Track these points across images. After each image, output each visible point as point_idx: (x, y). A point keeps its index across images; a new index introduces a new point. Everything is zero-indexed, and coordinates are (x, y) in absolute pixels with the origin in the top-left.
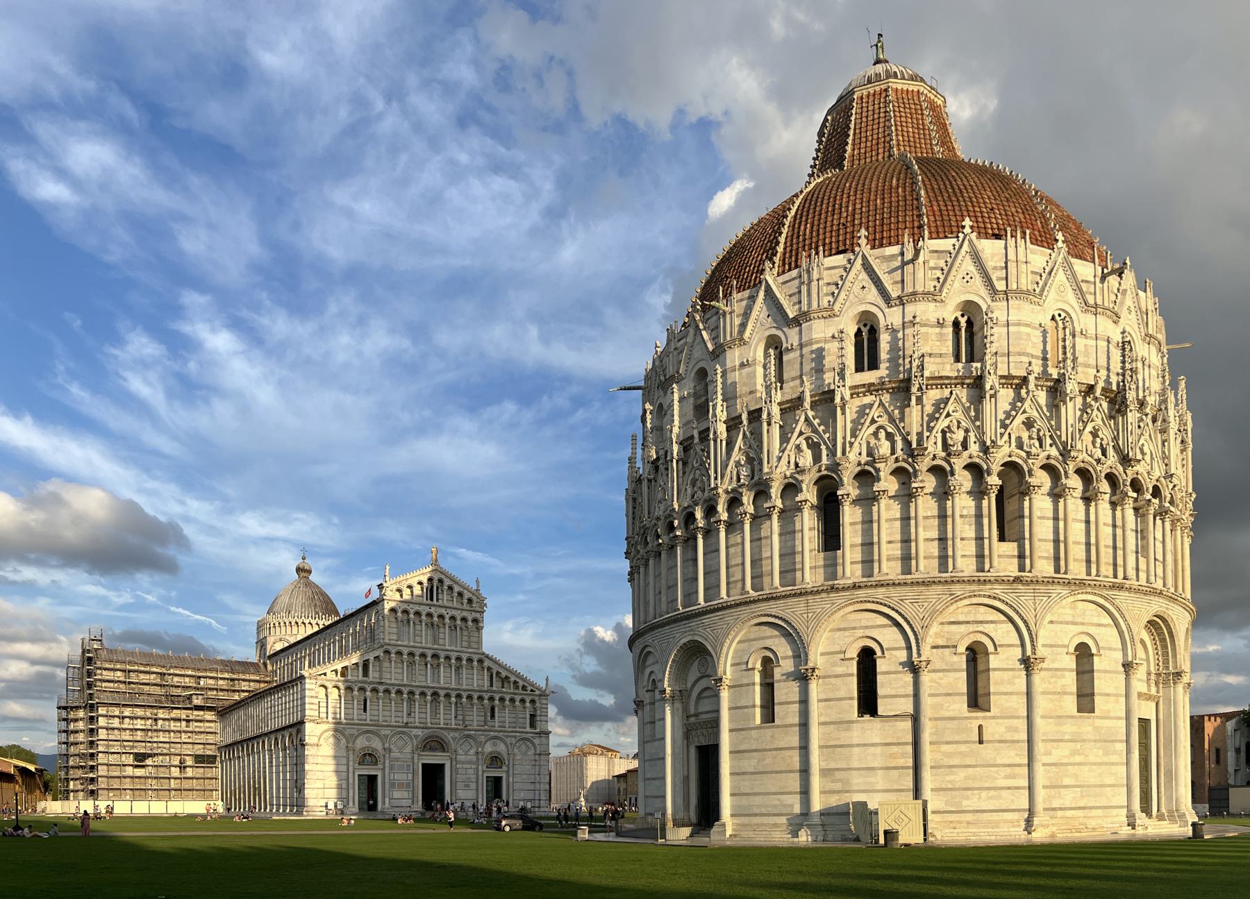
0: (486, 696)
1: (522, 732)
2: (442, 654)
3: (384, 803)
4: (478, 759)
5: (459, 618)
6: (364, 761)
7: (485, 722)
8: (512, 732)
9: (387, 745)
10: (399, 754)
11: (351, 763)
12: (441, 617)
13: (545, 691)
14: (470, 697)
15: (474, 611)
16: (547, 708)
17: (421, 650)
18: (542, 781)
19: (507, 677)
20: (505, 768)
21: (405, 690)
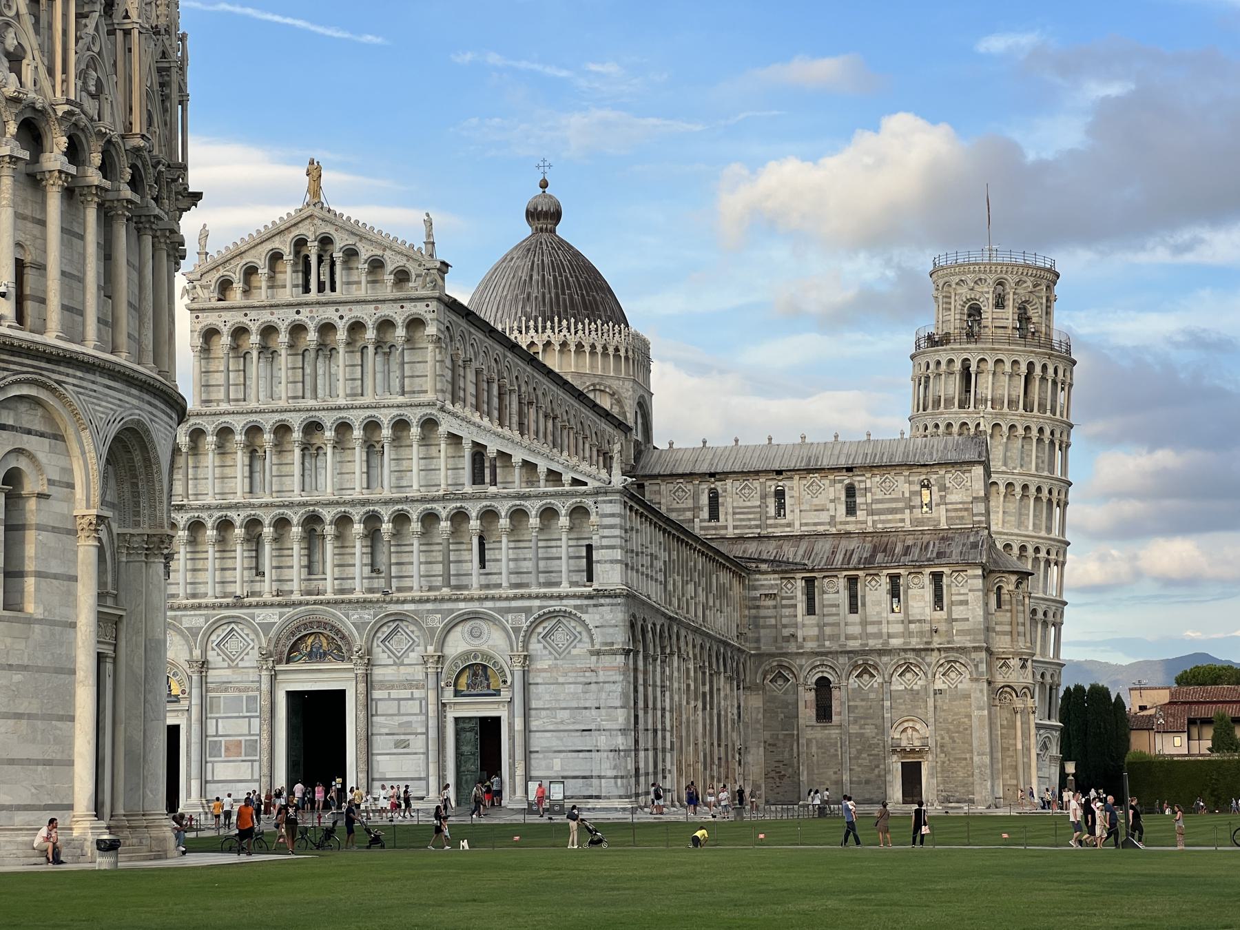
0: (443, 510)
1: (545, 597)
3: (189, 795)
5: (370, 324)
8: (515, 598)
10: (228, 672)
17: (277, 417)
20: (505, 694)
21: (238, 518)
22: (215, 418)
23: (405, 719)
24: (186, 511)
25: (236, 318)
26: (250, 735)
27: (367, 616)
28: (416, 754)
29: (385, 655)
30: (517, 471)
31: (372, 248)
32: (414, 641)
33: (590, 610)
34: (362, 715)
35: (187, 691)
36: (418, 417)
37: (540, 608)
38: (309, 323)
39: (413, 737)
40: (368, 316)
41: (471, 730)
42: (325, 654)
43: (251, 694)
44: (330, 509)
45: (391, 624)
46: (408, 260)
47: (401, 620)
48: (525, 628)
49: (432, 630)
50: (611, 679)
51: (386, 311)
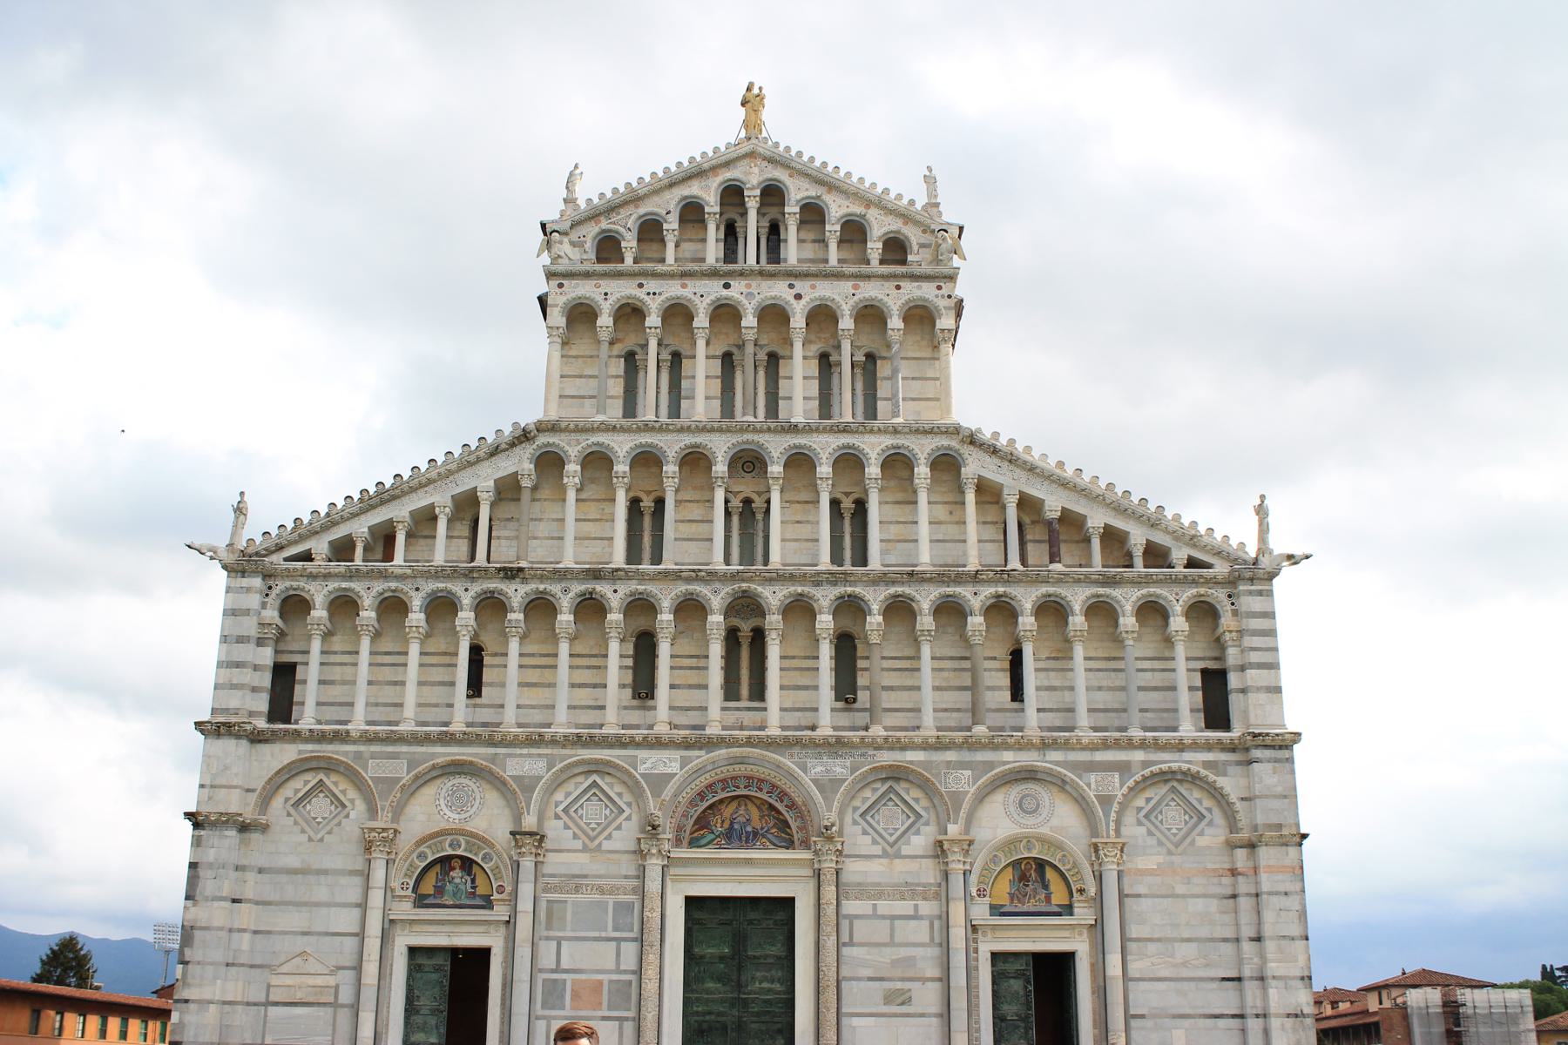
0: (976, 598)
2: (776, 448)
4: (946, 875)
6: (439, 891)
7: (975, 712)
10: (583, 858)
11: (376, 898)
12: (774, 315)
13: (1256, 562)
14: (900, 610)
15: (914, 277)
16: (1272, 633)
17: (689, 439)
18: (1273, 968)
19: (1071, 520)
20: (1083, 914)
21: (615, 596)
22: (584, 436)
23: (904, 952)
24: (525, 581)
25: (622, 290)
26: (618, 971)
27: (839, 770)
28: (922, 1015)
29: (868, 839)
30: (1096, 544)
31: (847, 203)
32: (919, 816)
33: (1231, 770)
34: (830, 943)
35: (508, 889)
36: (928, 450)
37: (1146, 764)
38: (745, 302)
40: (844, 296)
41: (1019, 975)
42: (755, 834)
43: (622, 898)
44: (776, 588)
45: (878, 785)
46: (906, 223)
47: (897, 779)
48: (1119, 798)
49: (957, 797)
50: (1282, 888)
51: (872, 291)
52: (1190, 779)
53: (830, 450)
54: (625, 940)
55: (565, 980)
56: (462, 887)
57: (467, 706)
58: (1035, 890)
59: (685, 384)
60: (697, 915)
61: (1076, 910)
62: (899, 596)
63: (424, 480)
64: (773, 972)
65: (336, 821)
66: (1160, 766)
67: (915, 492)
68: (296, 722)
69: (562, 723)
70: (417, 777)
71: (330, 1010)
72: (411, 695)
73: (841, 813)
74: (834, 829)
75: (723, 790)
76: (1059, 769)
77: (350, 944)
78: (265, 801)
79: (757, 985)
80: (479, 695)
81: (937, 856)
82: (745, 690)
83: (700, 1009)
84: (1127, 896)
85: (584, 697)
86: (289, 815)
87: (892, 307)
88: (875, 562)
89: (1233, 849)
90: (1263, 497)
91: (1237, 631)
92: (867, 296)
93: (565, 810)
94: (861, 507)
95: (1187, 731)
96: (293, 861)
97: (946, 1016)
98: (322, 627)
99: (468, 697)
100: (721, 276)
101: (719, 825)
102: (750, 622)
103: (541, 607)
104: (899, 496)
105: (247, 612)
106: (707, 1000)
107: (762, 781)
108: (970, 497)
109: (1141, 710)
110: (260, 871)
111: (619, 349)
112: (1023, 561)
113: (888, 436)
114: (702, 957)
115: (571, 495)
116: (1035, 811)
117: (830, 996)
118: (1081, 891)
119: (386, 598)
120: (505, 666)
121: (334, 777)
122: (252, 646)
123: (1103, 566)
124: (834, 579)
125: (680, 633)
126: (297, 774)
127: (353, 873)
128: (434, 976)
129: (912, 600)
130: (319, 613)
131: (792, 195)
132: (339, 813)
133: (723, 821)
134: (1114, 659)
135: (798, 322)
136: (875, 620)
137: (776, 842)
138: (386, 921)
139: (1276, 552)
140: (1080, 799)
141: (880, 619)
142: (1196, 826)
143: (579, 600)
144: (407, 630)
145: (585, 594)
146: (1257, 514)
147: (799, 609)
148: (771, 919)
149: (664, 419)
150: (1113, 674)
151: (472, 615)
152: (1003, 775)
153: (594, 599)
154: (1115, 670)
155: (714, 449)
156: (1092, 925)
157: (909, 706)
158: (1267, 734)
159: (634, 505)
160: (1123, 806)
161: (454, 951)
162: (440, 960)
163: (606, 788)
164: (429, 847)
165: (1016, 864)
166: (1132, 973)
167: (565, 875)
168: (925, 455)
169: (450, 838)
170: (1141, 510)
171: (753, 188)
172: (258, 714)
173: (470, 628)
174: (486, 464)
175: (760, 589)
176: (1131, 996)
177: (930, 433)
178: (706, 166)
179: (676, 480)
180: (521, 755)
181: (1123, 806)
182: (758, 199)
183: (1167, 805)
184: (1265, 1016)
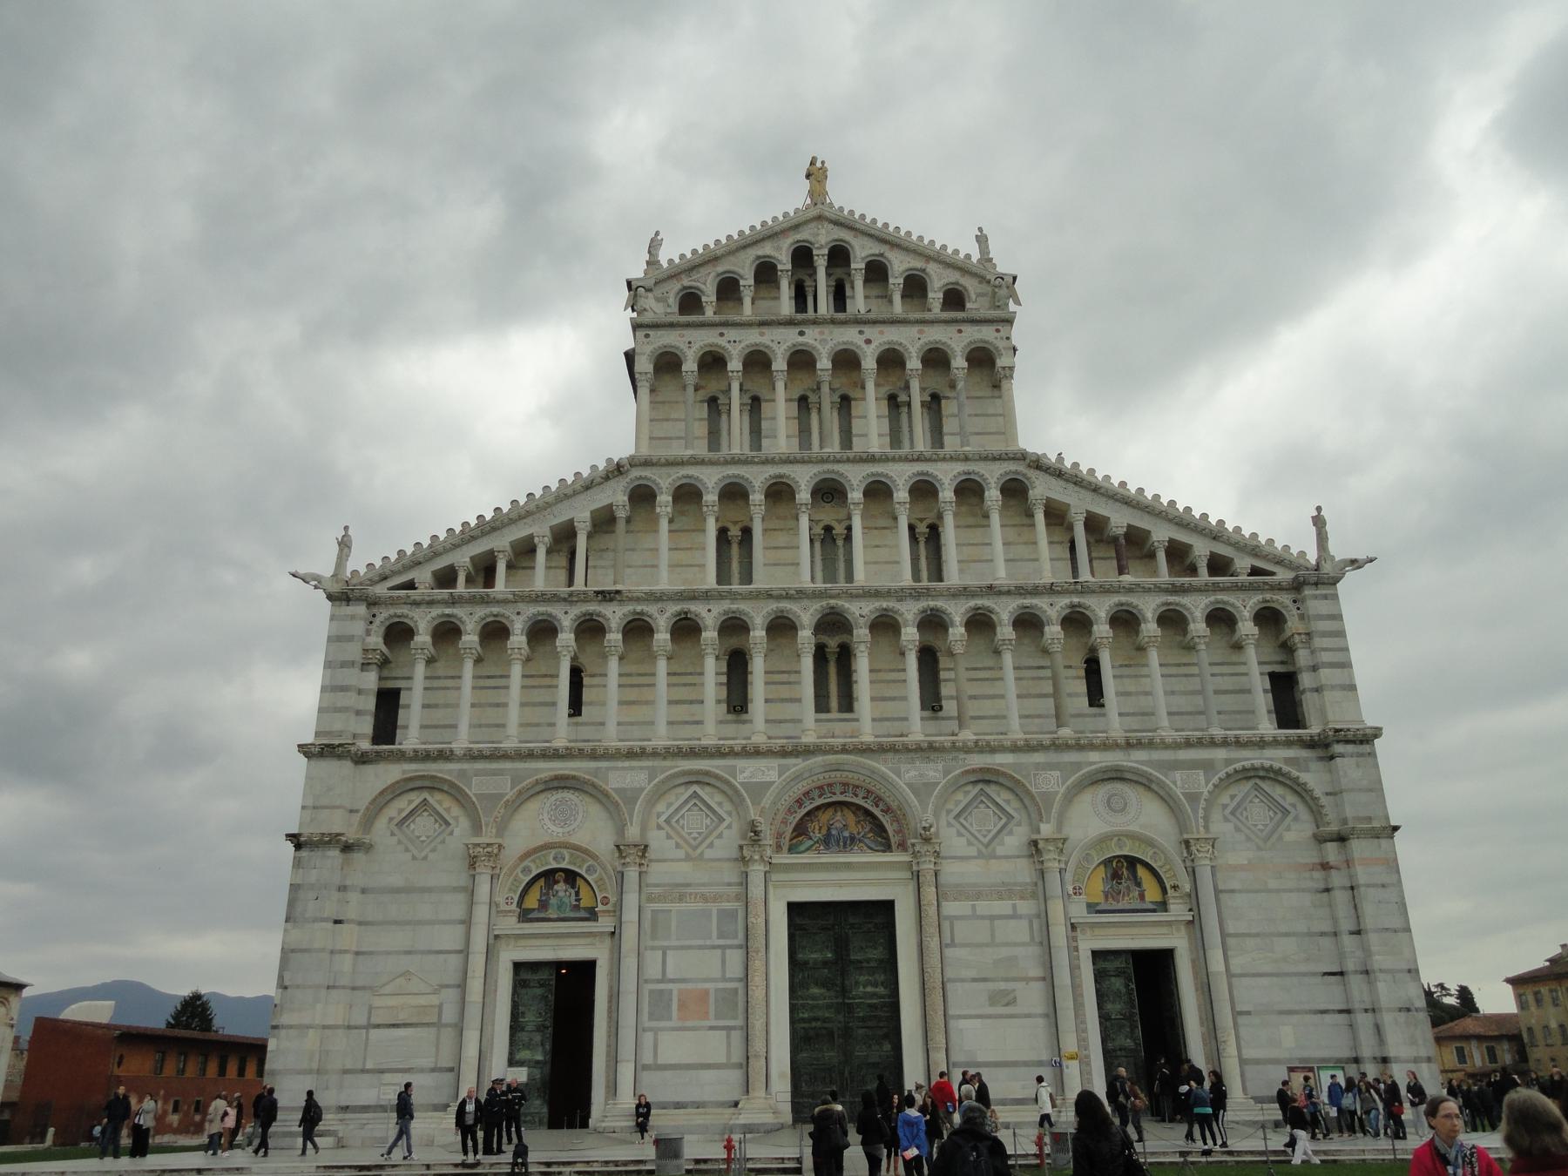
0: (1052, 609)
1: (1238, 743)
2: (856, 479)
3: (613, 1089)
4: (1042, 873)
6: (543, 905)
7: (1059, 717)
9: (633, 833)
10: (685, 867)
11: (481, 913)
13: (1317, 568)
14: (980, 623)
16: (1341, 634)
18: (1379, 961)
20: (1178, 910)
21: (710, 616)
23: (1005, 952)
25: (702, 339)
26: (724, 979)
27: (932, 773)
28: (1028, 1016)
29: (963, 841)
30: (1161, 556)
32: (1010, 817)
33: (1314, 766)
35: (613, 899)
36: (997, 475)
37: (1228, 762)
38: (819, 347)
39: (1019, 985)
40: (912, 342)
42: (852, 839)
44: (863, 604)
45: (969, 788)
46: (963, 276)
47: (988, 782)
49: (1048, 797)
52: (1272, 775)
53: (906, 477)
54: (730, 947)
55: (671, 990)
56: (566, 900)
57: (569, 725)
58: (1128, 888)
59: (765, 425)
60: (798, 921)
61: (1172, 907)
62: (979, 608)
63: (523, 513)
64: (877, 976)
65: (441, 838)
66: (1242, 763)
67: (986, 516)
68: (400, 744)
69: (661, 737)
70: (520, 793)
71: (433, 1030)
72: (514, 715)
73: (936, 814)
74: (932, 830)
75: (820, 796)
76: (1145, 768)
77: (454, 961)
78: (368, 821)
79: (861, 989)
80: (580, 715)
81: (1032, 856)
82: (834, 702)
83: (806, 1015)
84: (1221, 891)
85: (682, 712)
86: (393, 834)
87: (956, 349)
88: (953, 575)
89: (1326, 841)
90: (1319, 509)
91: (1305, 634)
92: (932, 339)
93: (667, 821)
94: (934, 532)
95: (1266, 729)
96: (396, 880)
97: (1052, 1015)
98: (426, 651)
99: (570, 715)
100: (795, 324)
101: (817, 831)
102: (837, 638)
103: (638, 629)
104: (971, 521)
105: (350, 639)
106: (813, 1007)
107: (857, 787)
108: (1040, 517)
109: (1219, 713)
110: (364, 891)
111: (702, 394)
112: (1093, 574)
113: (959, 463)
114: (806, 963)
115: (664, 525)
116: (1123, 810)
117: (936, 998)
118: (1175, 887)
119: (487, 624)
120: (605, 686)
121: (438, 796)
122: (356, 670)
123: (1170, 576)
124: (916, 594)
125: (772, 650)
126: (399, 795)
127: (456, 889)
128: (539, 991)
129: (990, 612)
130: (423, 638)
131: (858, 253)
132: (443, 831)
133: (820, 830)
134: (1185, 665)
135: (869, 363)
136: (957, 632)
137: (873, 846)
138: (492, 937)
139: (1337, 559)
140: (1166, 797)
141: (963, 630)
142: (1283, 819)
143: (675, 619)
144: (509, 652)
145: (680, 614)
146: (1315, 524)
147: (885, 625)
148: (870, 923)
149: (747, 451)
150: (1184, 679)
151: (572, 636)
152: (1090, 774)
153: (689, 619)
154: (1186, 675)
155: (797, 479)
156: (1190, 921)
157: (993, 713)
158: (1349, 730)
159: (722, 533)
160: (1210, 803)
161: (558, 965)
162: (544, 975)
163: (706, 798)
164: (534, 861)
165: (1107, 863)
166: (1235, 969)
167: (669, 885)
168: (995, 479)
169: (553, 852)
170: (1203, 524)
171: (821, 247)
172: (363, 736)
173: (571, 649)
174: (582, 497)
175: (847, 605)
176: (1235, 993)
177: (999, 459)
178: (777, 229)
179: (763, 507)
180: (624, 768)
181: (1210, 803)
182: (826, 257)
183: (1251, 802)
184: (1374, 1010)
